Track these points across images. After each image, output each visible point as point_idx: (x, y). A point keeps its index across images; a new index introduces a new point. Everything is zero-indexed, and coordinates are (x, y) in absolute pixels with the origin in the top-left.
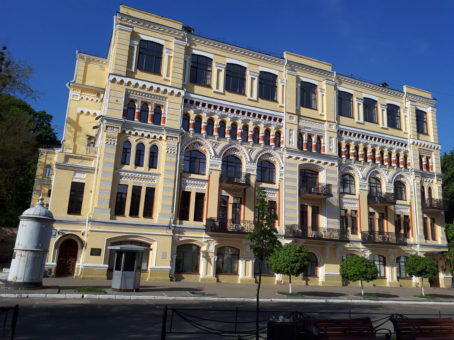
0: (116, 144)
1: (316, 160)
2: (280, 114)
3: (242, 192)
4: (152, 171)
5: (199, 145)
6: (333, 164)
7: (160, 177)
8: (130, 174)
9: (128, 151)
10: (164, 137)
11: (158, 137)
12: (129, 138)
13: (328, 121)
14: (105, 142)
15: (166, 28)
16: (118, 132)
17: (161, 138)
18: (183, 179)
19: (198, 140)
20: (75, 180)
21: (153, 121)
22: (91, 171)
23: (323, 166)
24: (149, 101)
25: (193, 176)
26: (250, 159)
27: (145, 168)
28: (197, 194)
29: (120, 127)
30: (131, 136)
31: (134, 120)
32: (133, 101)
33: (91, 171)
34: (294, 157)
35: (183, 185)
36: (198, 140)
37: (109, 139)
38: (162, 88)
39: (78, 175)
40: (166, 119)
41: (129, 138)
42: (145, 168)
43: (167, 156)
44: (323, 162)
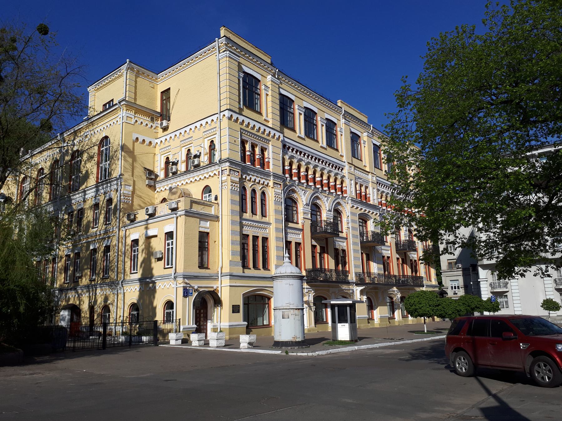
0: (238, 190)
1: (368, 210)
2: (343, 164)
3: (325, 241)
4: (264, 219)
7: (271, 227)
8: (250, 223)
14: (230, 187)
15: (259, 60)
20: (202, 230)
22: (216, 218)
23: (371, 215)
24: (257, 143)
27: (258, 217)
28: (296, 243)
33: (216, 218)
34: (356, 206)
37: (234, 184)
38: (268, 130)
39: (203, 223)
42: (258, 217)
43: (275, 204)
44: (372, 211)
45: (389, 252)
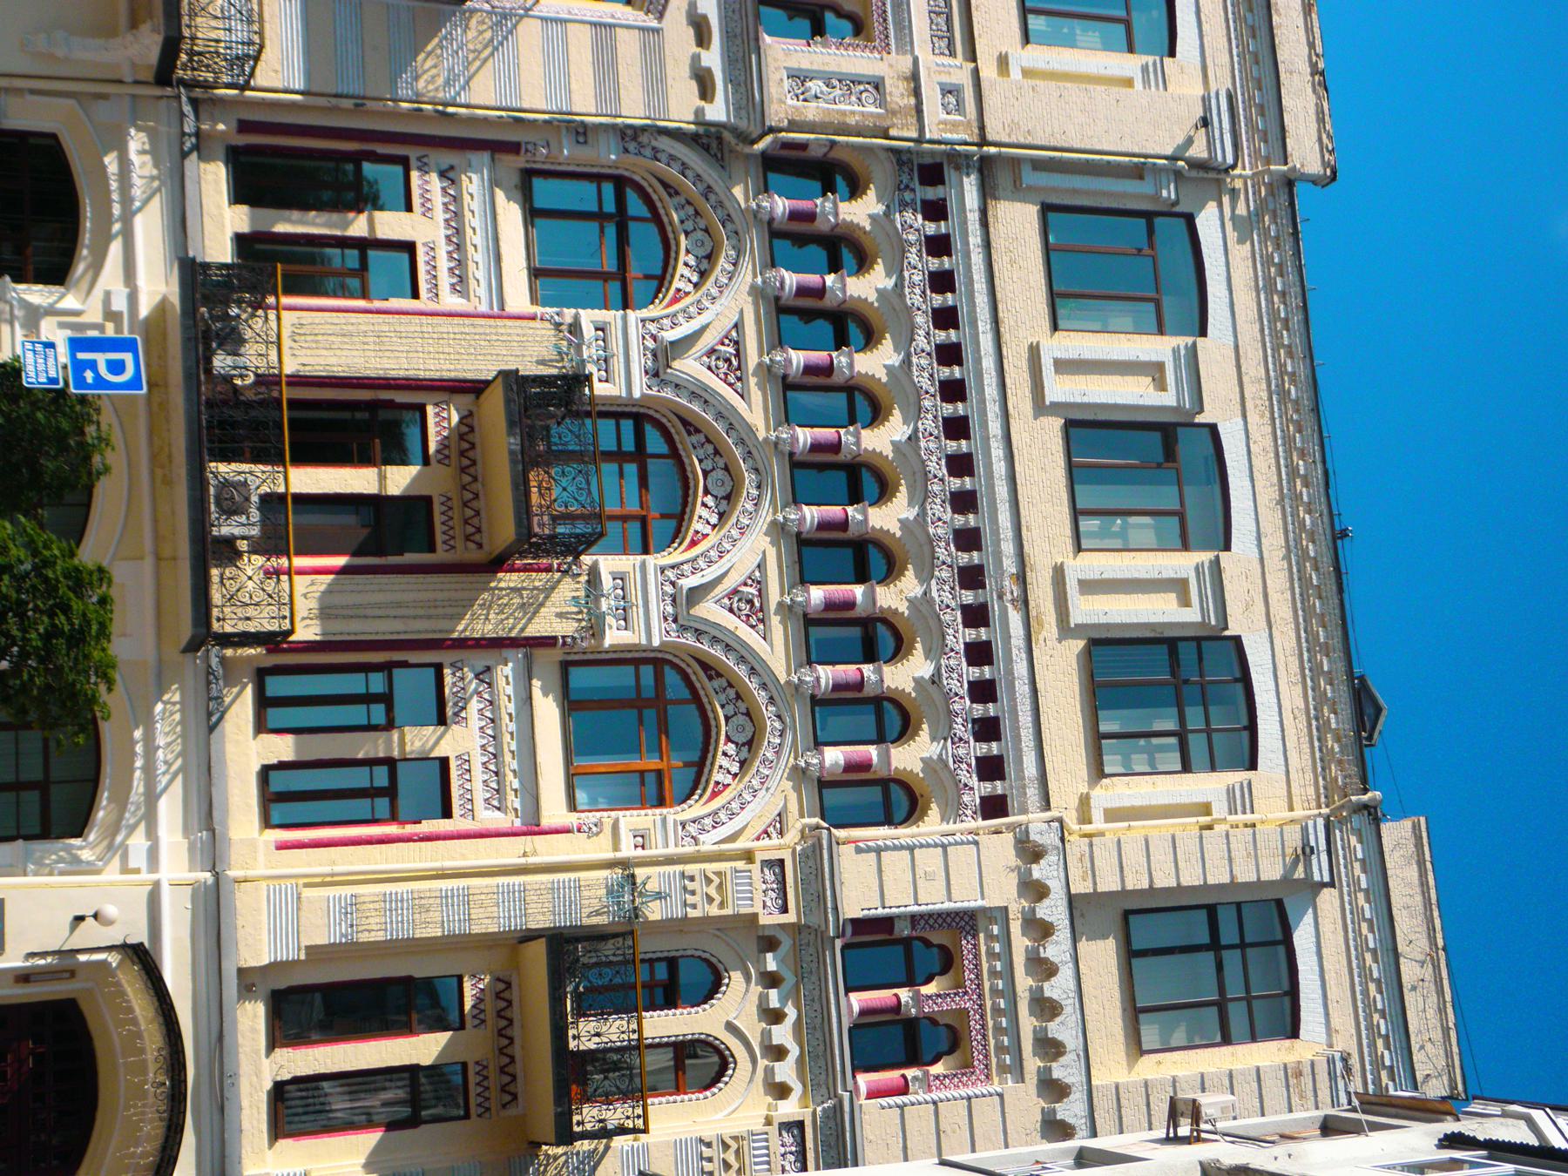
5: (728, 497)
6: (706, 92)
9: (646, 712)
10: (790, 1109)
11: (785, 1071)
12: (737, 976)
13: (976, 71)
16: (758, 908)
17: (782, 1091)
18: (485, 156)
19: (749, 478)
21: (868, 1026)
25: (547, 712)
26: (696, 594)
29: (791, 917)
30: (756, 990)
31: (848, 990)
32: (947, 962)
35: (447, 158)
36: (749, 478)
40: (899, 1100)
41: (737, 976)
45: (450, 301)
